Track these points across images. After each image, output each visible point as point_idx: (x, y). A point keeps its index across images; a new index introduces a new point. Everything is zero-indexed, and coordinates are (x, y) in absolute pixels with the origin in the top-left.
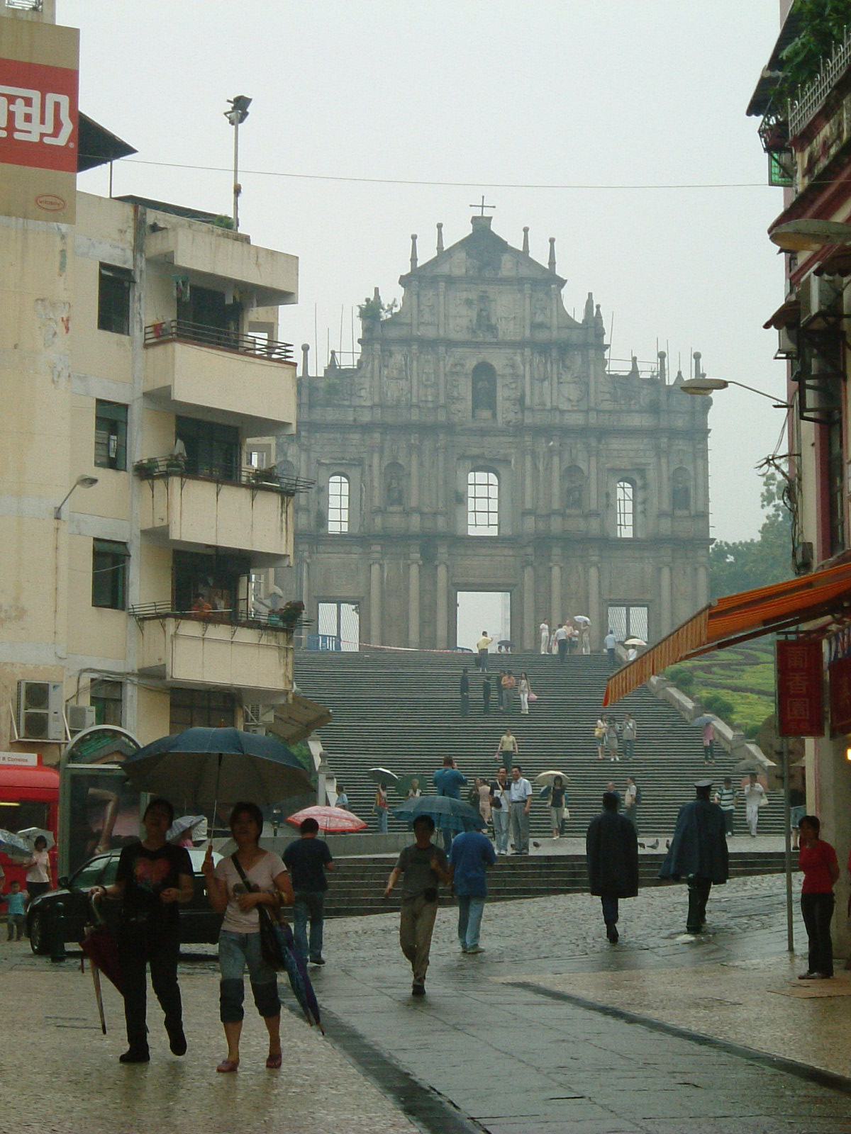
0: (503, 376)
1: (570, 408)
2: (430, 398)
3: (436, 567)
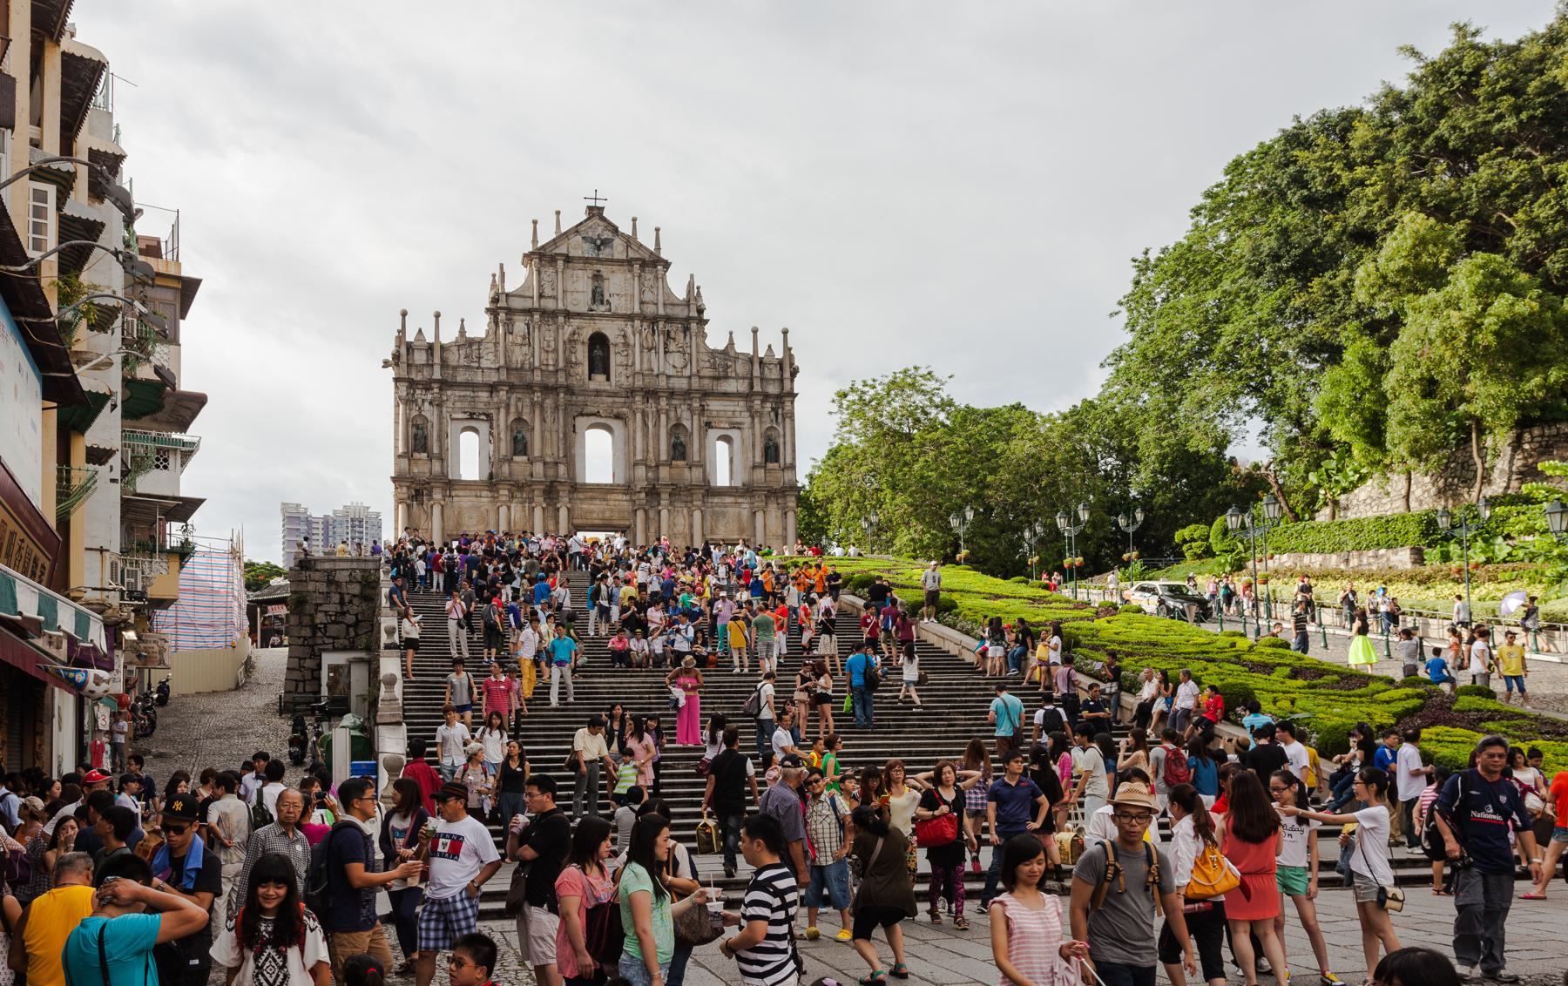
0: (616, 345)
2: (551, 362)
3: (558, 509)
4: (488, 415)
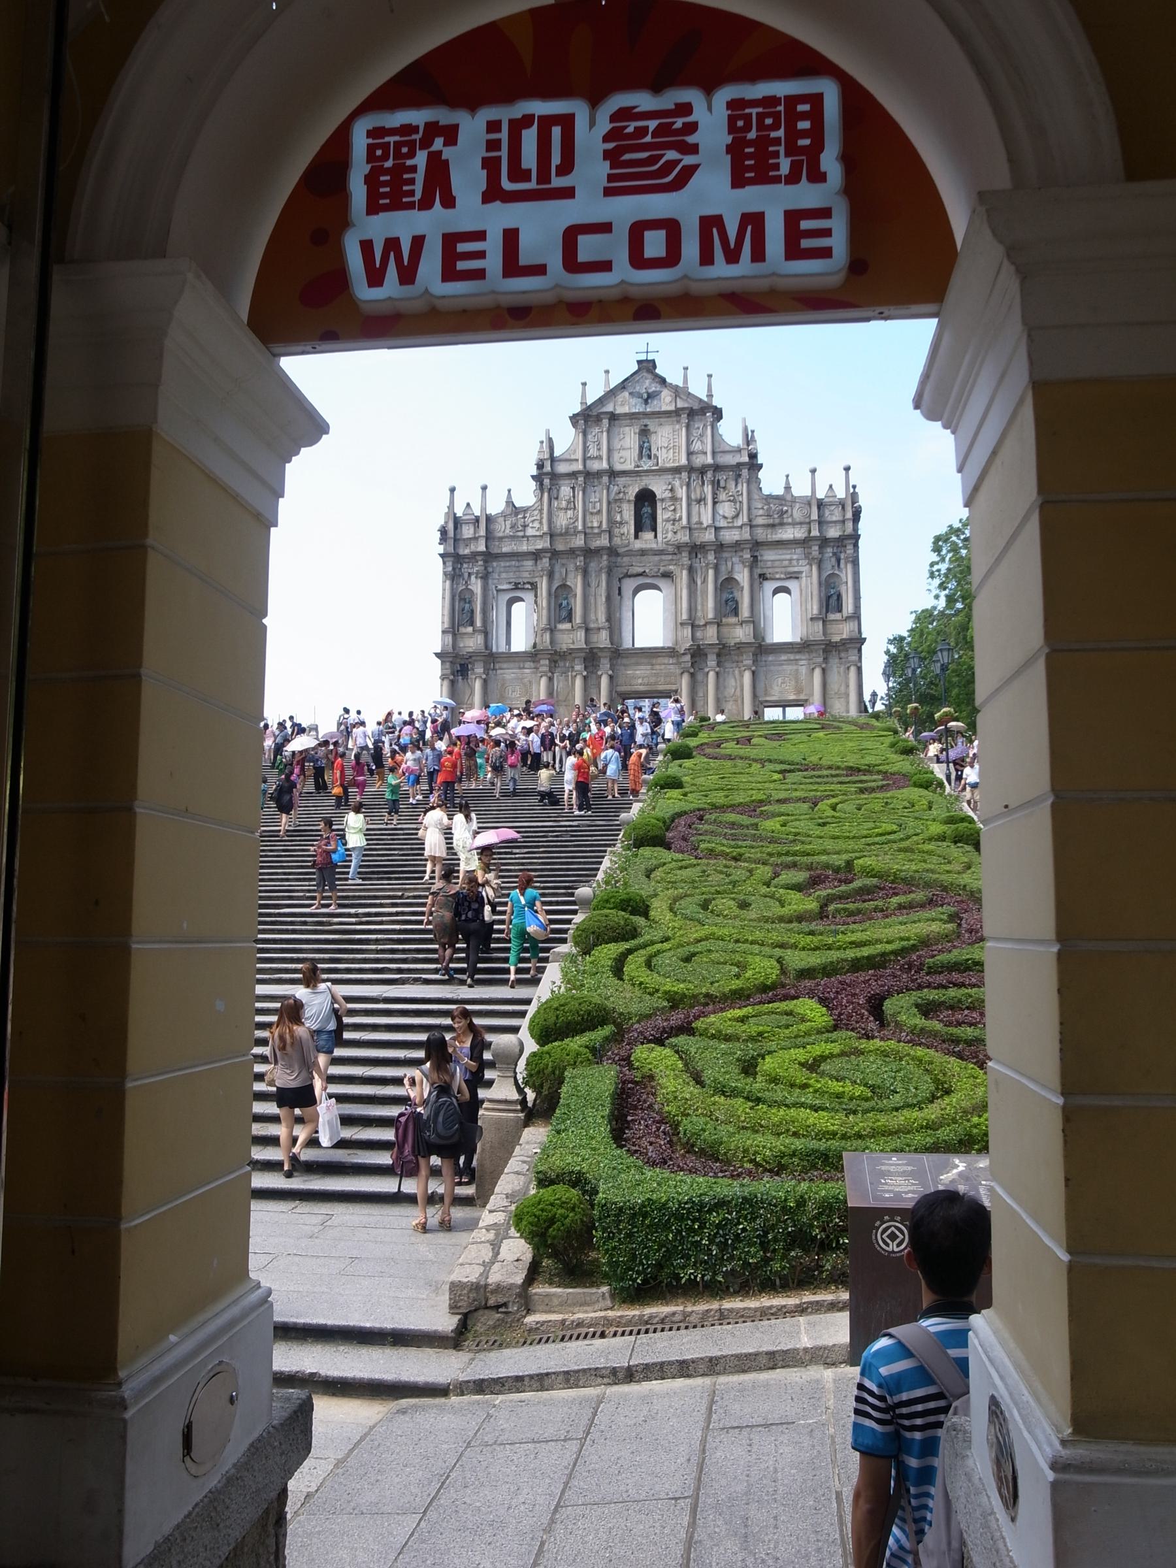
0: (663, 500)
1: (726, 525)
2: (595, 524)
3: (600, 677)
4: (531, 584)
